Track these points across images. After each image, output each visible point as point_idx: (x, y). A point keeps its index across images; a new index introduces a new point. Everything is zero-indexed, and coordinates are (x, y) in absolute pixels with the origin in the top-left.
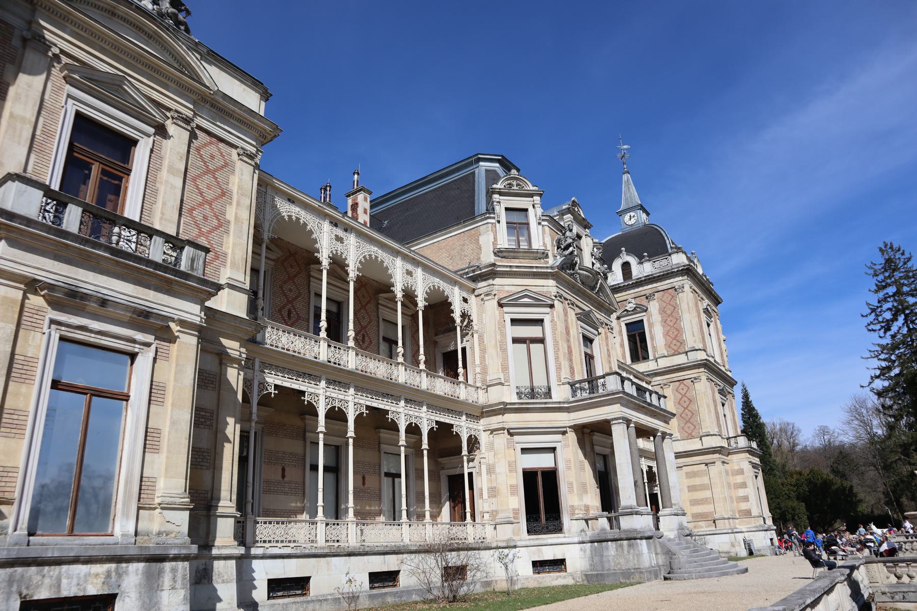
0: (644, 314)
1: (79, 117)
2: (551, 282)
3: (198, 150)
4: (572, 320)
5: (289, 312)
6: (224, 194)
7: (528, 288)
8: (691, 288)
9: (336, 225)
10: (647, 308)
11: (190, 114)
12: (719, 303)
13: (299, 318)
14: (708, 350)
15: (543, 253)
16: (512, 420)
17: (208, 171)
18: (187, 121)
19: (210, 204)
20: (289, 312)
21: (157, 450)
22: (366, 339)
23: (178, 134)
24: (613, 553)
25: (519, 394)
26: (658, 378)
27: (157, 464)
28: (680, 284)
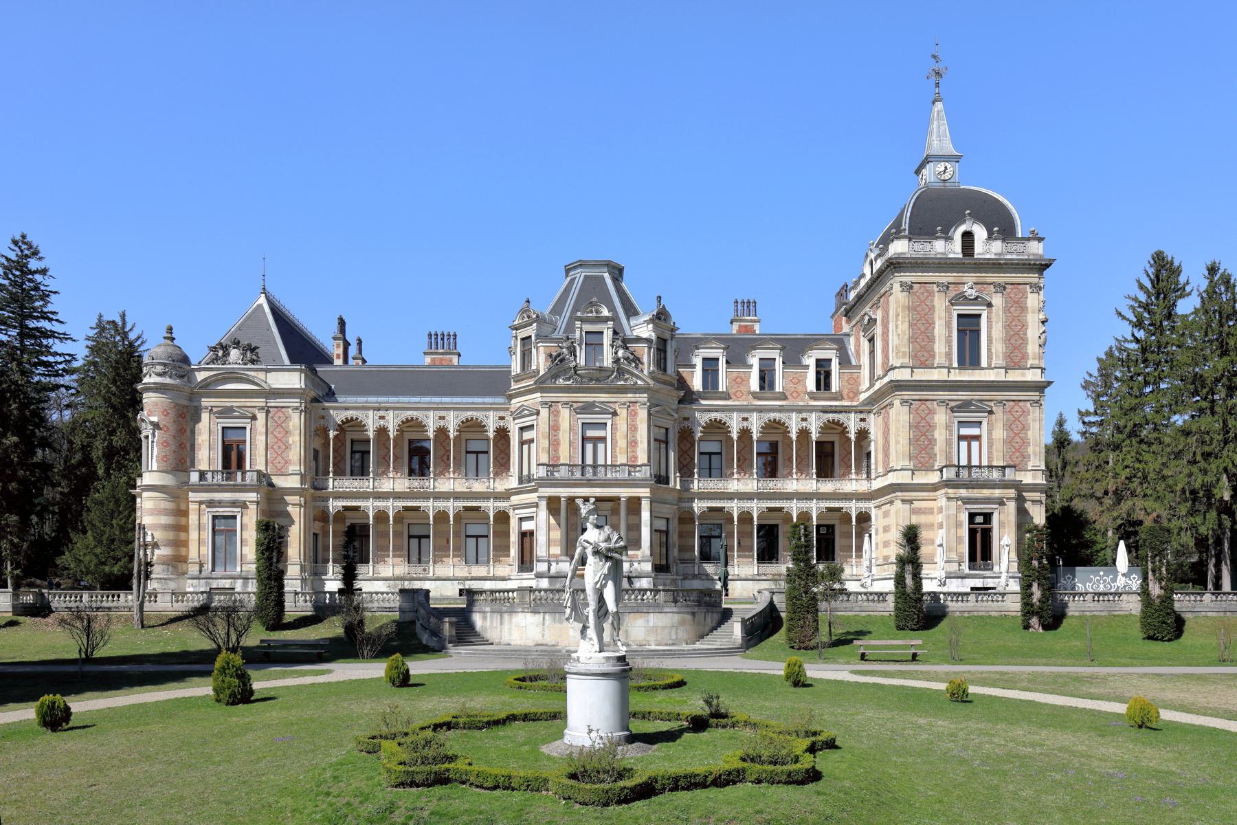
2: (539, 395)
3: (272, 418)
4: (563, 417)
6: (287, 432)
7: (525, 404)
8: (901, 286)
9: (379, 410)
11: (264, 404)
12: (1048, 266)
16: (515, 499)
17: (279, 425)
18: (263, 408)
23: (261, 417)
24: (737, 589)
25: (521, 482)
27: (246, 550)
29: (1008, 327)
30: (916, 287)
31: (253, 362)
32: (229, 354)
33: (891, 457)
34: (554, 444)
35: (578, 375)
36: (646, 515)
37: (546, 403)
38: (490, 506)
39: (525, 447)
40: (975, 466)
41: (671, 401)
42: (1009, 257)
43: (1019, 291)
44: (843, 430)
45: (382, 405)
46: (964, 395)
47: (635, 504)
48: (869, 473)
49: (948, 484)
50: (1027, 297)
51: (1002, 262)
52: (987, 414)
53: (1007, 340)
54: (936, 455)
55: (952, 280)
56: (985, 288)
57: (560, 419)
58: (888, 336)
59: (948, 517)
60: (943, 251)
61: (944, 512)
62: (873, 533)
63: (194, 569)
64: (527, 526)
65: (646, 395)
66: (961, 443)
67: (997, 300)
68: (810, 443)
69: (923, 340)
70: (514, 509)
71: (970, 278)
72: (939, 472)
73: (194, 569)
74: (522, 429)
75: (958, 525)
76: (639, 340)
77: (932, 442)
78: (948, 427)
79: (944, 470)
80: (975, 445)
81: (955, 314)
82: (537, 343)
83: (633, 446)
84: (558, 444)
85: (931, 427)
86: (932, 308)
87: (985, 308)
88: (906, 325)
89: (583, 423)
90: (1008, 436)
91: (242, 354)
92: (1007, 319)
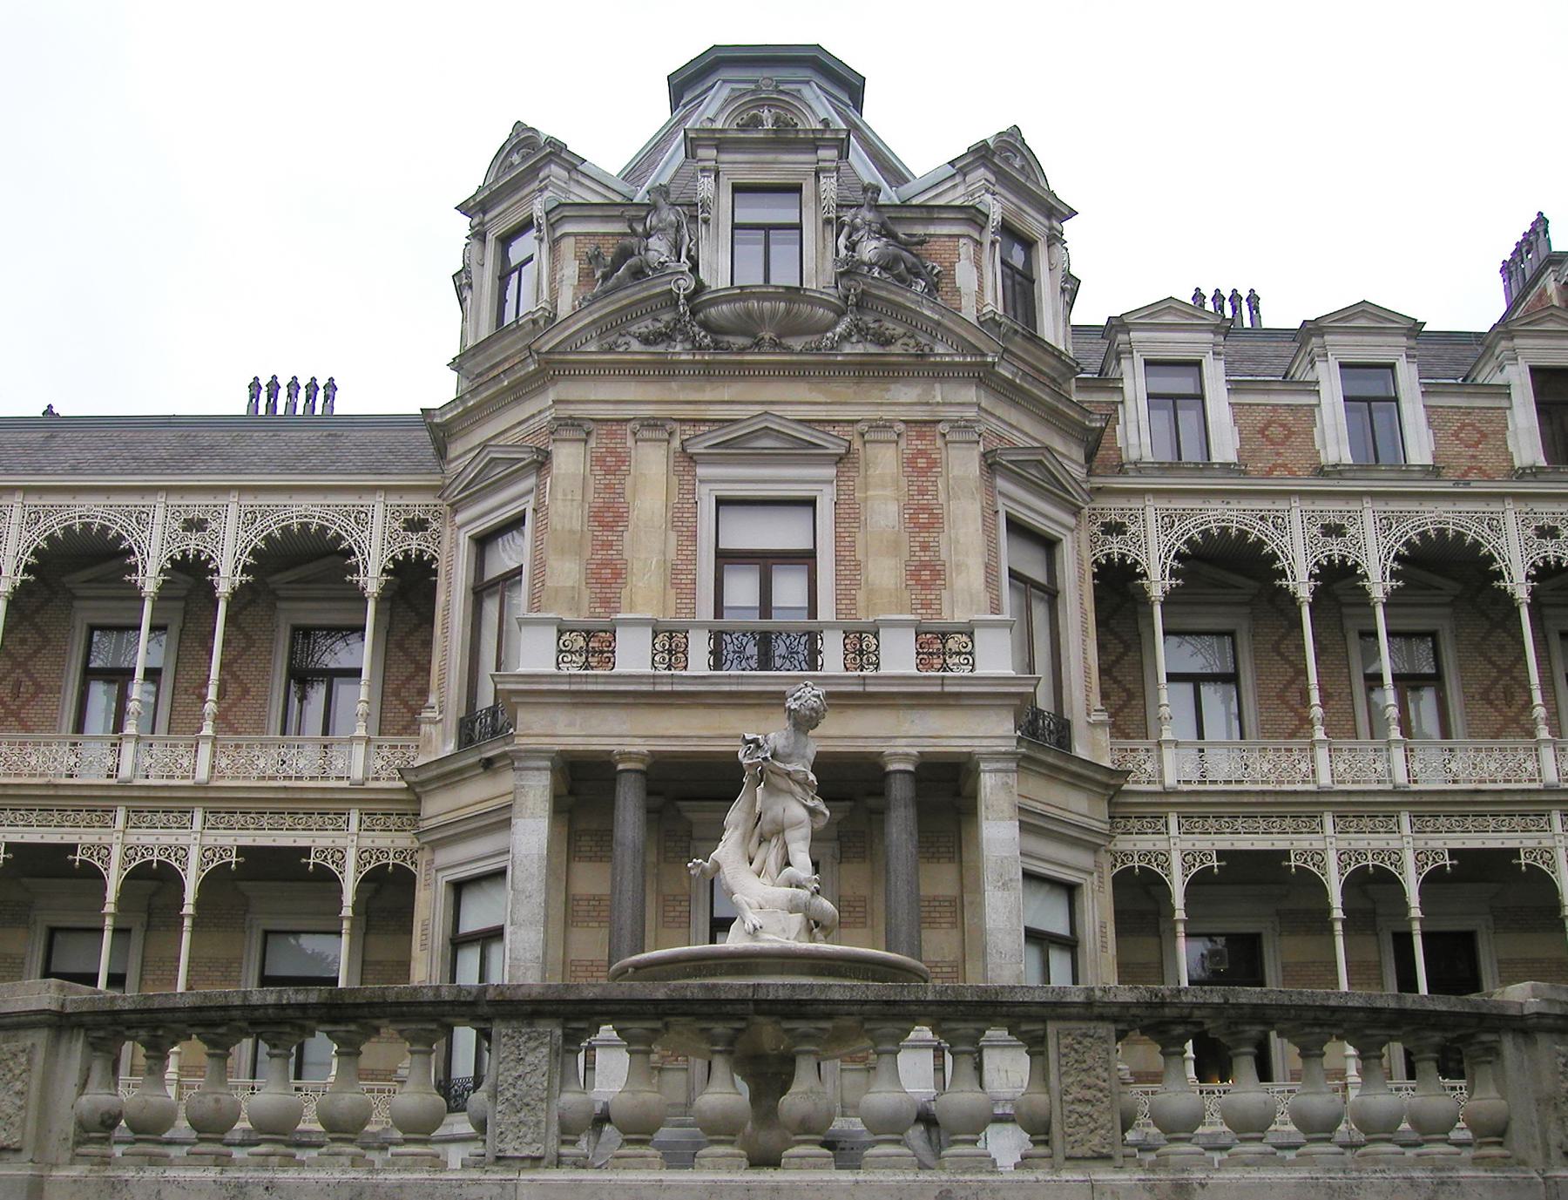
13: (39, 688)
15: (535, 322)
37: (573, 423)
39: (491, 607)
65: (970, 394)
82: (552, 226)
83: (925, 586)
89: (721, 502)
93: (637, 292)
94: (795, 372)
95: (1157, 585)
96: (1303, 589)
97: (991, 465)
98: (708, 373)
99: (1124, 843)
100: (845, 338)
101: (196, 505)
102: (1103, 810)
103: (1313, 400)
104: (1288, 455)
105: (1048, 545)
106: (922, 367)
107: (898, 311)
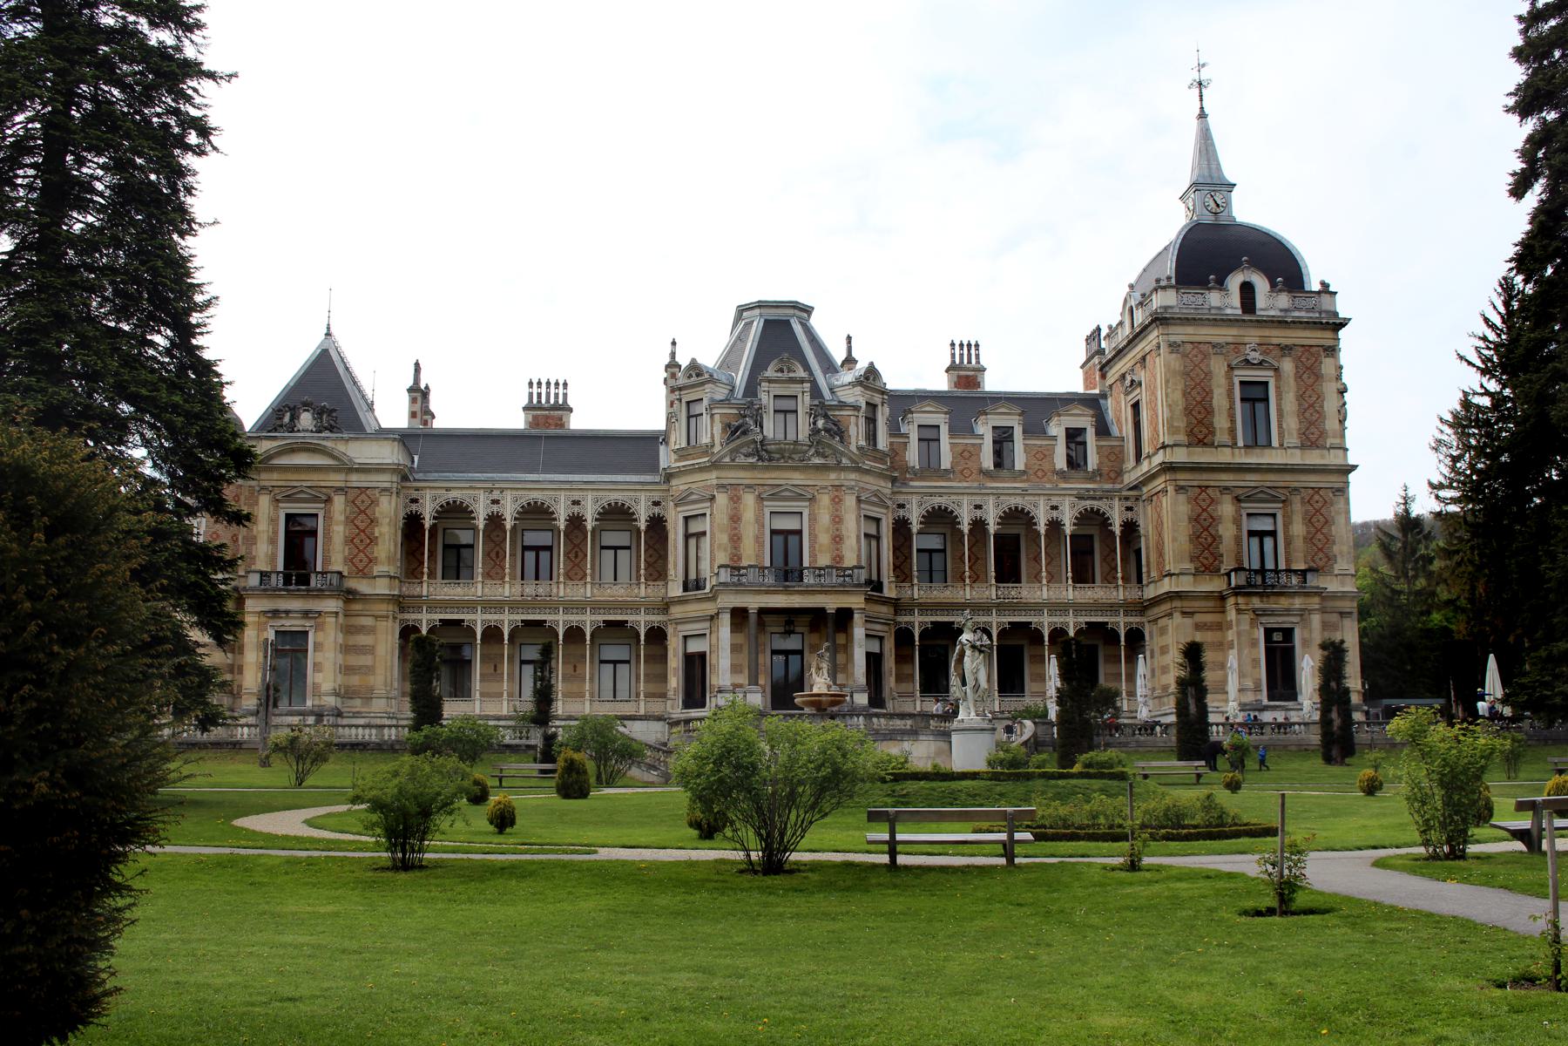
0: (1138, 391)
1: (287, 514)
5: (497, 553)
6: (373, 521)
10: (1140, 384)
11: (342, 484)
14: (1222, 437)
16: (677, 611)
17: (362, 512)
18: (339, 490)
19: (363, 531)
20: (497, 553)
21: (320, 671)
22: (580, 553)
25: (686, 589)
26: (1145, 489)
28: (1154, 342)
29: (1300, 397)
30: (1189, 347)
31: (331, 429)
32: (298, 417)
33: (1167, 558)
34: (736, 539)
35: (766, 451)
36: (859, 632)
37: (723, 486)
38: (642, 621)
39: (692, 542)
40: (1269, 570)
41: (883, 484)
42: (1296, 314)
43: (1312, 354)
44: (1103, 521)
45: (497, 486)
46: (1252, 479)
47: (844, 618)
48: (1140, 580)
49: (1238, 591)
50: (1321, 363)
51: (1289, 320)
52: (1281, 505)
53: (1301, 413)
54: (1222, 555)
55: (1230, 340)
56: (1271, 351)
57: (742, 506)
58: (1156, 405)
59: (1239, 634)
60: (1218, 305)
61: (1235, 628)
62: (1148, 653)
63: (249, 702)
64: (694, 647)
65: (853, 476)
66: (1251, 539)
67: (1287, 366)
68: (1063, 538)
69: (1199, 413)
70: (676, 624)
71: (1252, 336)
72: (1226, 577)
73: (249, 702)
74: (686, 519)
75: (1254, 644)
76: (842, 405)
77: (1216, 539)
78: (1237, 522)
79: (1233, 574)
80: (1268, 542)
81: (1236, 381)
82: (711, 409)
83: (837, 543)
84: (739, 539)
85: (1215, 520)
86: (1211, 372)
87: (1271, 373)
88: (1178, 396)
90: (1308, 533)
91: (314, 419)
92: (1299, 389)
93: (744, 439)
94: (795, 469)
95: (915, 527)
96: (966, 528)
97: (859, 500)
98: (767, 468)
99: (900, 619)
100: (813, 455)
101: (576, 496)
102: (892, 610)
103: (981, 441)
104: (970, 464)
105: (878, 520)
106: (839, 467)
107: (830, 446)
